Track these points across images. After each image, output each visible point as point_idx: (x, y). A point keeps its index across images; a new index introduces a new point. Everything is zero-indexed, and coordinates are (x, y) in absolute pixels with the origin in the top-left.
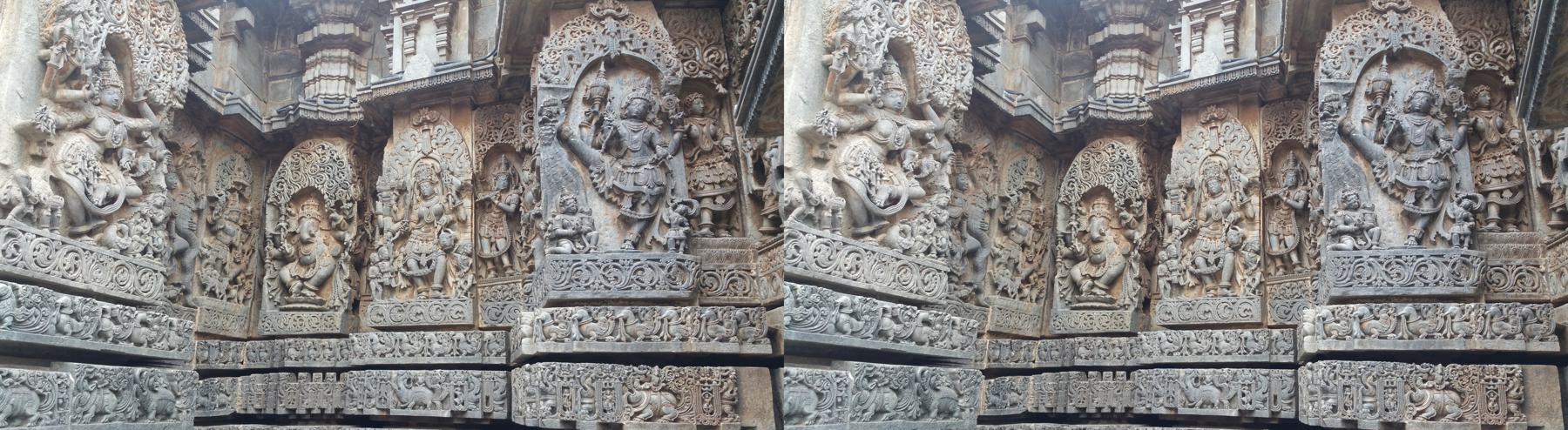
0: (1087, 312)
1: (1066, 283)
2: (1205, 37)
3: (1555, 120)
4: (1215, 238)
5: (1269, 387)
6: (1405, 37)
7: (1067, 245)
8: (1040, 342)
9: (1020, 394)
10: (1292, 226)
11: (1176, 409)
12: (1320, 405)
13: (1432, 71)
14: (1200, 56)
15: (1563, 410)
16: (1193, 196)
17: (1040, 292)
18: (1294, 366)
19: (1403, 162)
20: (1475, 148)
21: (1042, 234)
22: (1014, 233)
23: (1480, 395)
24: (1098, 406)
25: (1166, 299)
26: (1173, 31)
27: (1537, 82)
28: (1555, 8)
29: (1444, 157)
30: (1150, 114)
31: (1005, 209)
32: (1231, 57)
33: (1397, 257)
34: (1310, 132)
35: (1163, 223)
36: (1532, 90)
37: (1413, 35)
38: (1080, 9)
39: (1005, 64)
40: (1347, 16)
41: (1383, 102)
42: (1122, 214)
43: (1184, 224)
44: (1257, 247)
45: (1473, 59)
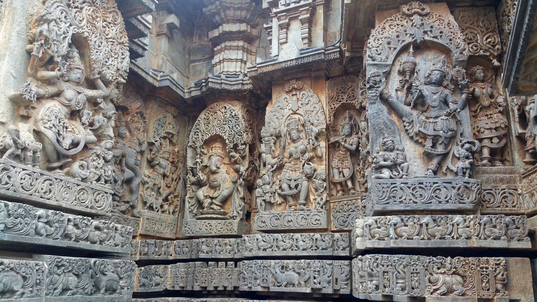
0: (208, 221)
1: (193, 201)
2: (288, 32)
3: (528, 90)
4: (295, 171)
5: (332, 272)
6: (425, 32)
7: (194, 175)
8: (175, 242)
9: (161, 278)
10: (348, 162)
11: (268, 288)
12: (367, 285)
13: (444, 56)
14: (284, 46)
15: (534, 288)
16: (280, 142)
17: (176, 208)
18: (349, 258)
19: (424, 118)
20: (473, 109)
21: (177, 167)
22: (157, 167)
23: (477, 278)
24: (215, 285)
25: (262, 212)
26: (267, 29)
27: (516, 63)
28: (528, 12)
29: (452, 115)
30: (251, 86)
31: (151, 150)
32: (306, 46)
33: (420, 183)
34: (360, 98)
35: (260, 161)
36: (512, 69)
37: (431, 31)
38: (202, 14)
39: (152, 51)
40: (386, 18)
41: (410, 77)
42: (231, 154)
43: (274, 161)
44: (324, 177)
45: (472, 48)
